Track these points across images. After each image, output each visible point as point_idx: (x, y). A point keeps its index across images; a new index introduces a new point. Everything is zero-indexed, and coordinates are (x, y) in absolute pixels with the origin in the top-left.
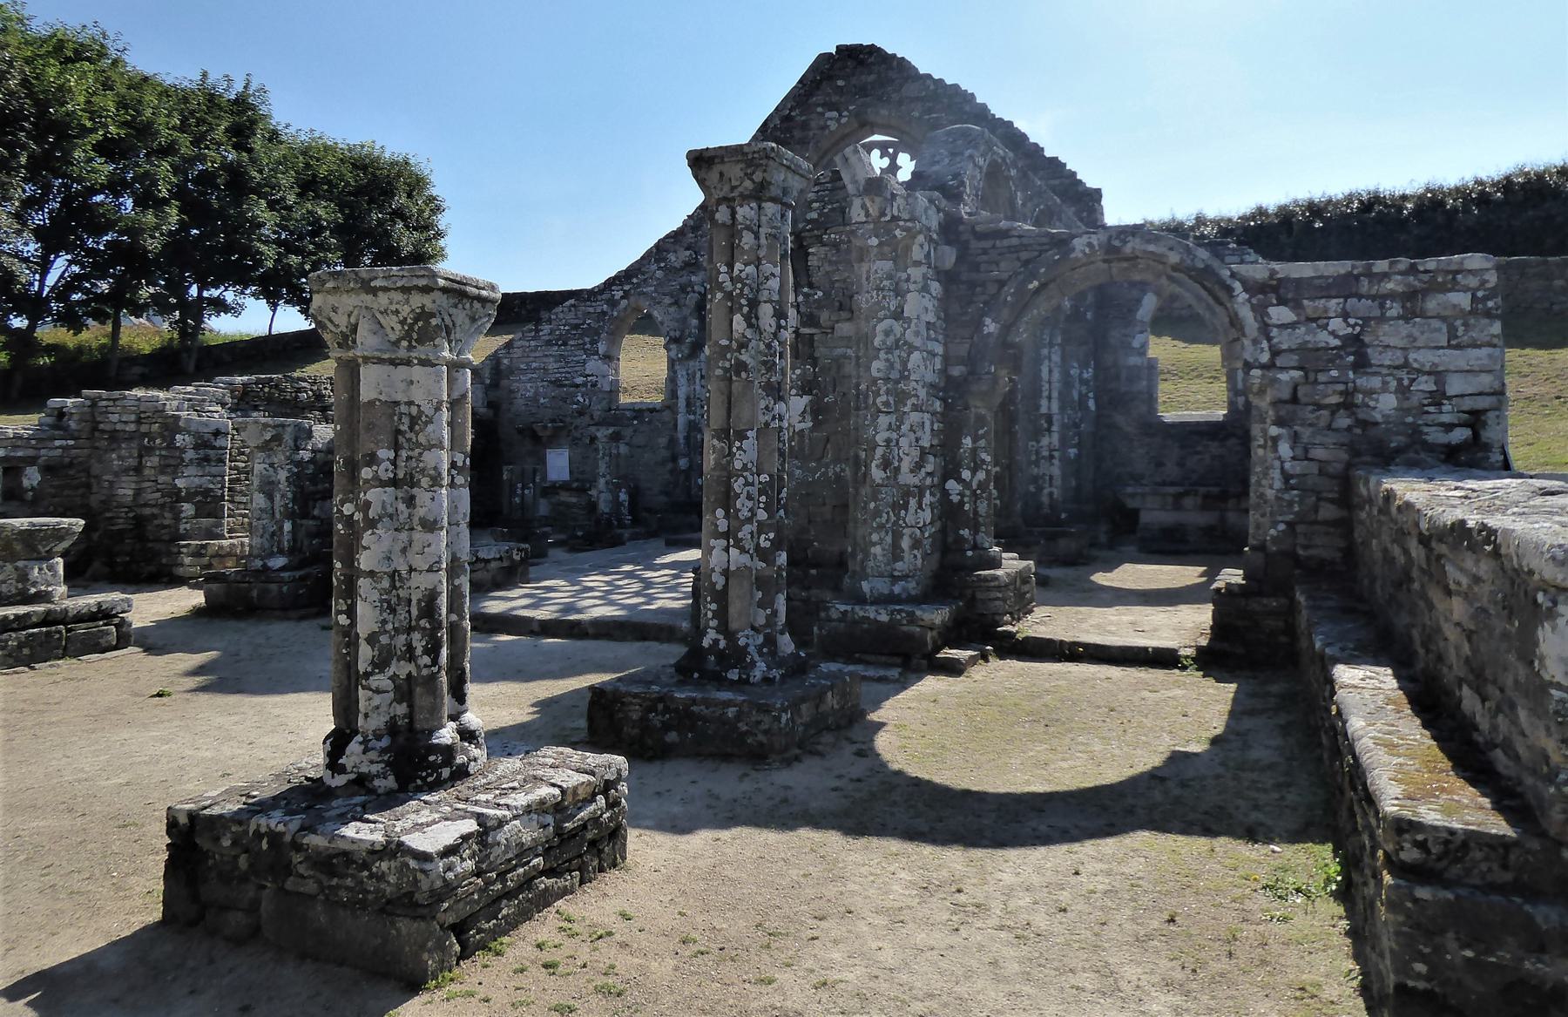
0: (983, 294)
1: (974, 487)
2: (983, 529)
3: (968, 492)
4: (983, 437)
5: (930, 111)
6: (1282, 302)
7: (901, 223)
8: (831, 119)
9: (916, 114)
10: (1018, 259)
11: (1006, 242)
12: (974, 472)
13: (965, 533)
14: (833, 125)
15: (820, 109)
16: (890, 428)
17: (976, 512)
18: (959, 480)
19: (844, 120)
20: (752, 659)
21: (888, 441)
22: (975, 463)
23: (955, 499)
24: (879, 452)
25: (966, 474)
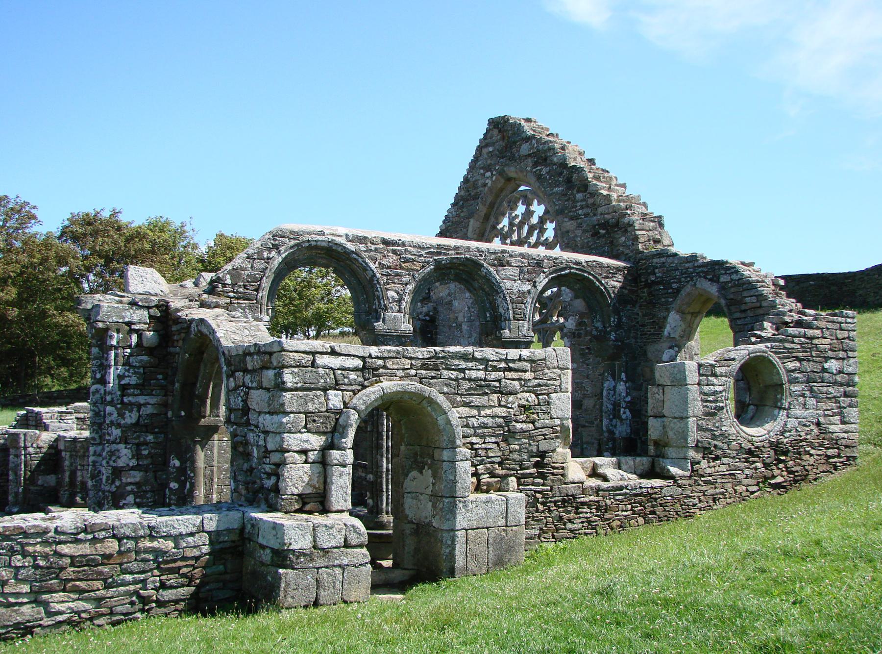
5: (536, 164)
8: (488, 178)
9: (529, 169)
14: (489, 182)
15: (482, 171)
16: (95, 454)
19: (494, 178)
21: (94, 462)
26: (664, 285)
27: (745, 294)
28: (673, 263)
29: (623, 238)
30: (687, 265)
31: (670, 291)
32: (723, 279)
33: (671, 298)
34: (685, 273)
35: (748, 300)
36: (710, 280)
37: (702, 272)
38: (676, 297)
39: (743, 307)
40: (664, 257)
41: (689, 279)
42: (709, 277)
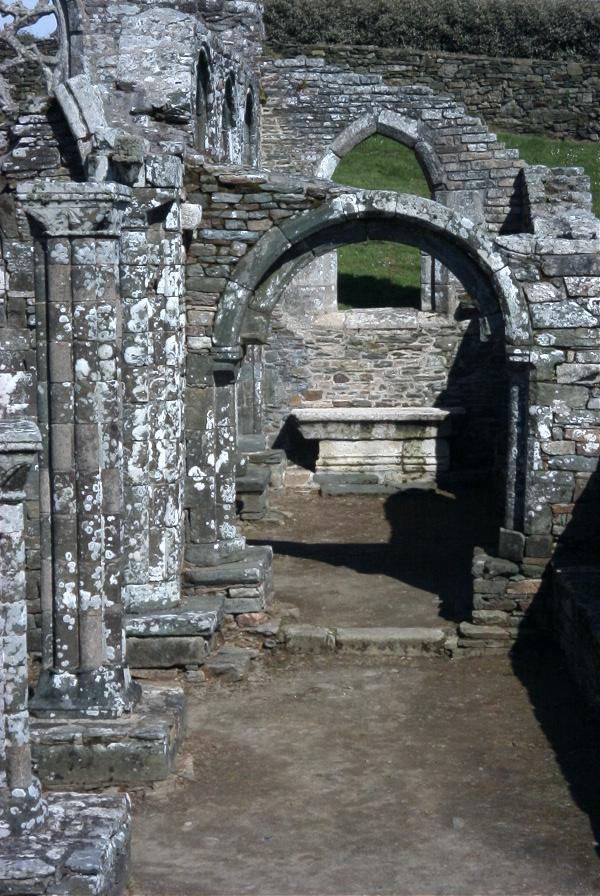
0: (229, 254)
1: (217, 471)
2: (227, 517)
3: (212, 479)
4: (226, 414)
6: (546, 278)
7: (158, 190)
10: (270, 218)
11: (257, 197)
12: (217, 455)
13: (213, 525)
17: (219, 499)
18: (204, 466)
20: (110, 693)
21: (145, 435)
22: (218, 443)
23: (200, 487)
24: (137, 447)
25: (211, 459)
26: (315, 114)
27: (466, 138)
28: (334, 82)
29: (229, 33)
30: (360, 89)
31: (326, 124)
32: (427, 115)
33: (329, 133)
34: (357, 100)
35: (472, 147)
36: (403, 114)
37: (390, 102)
38: (337, 133)
39: (463, 156)
40: (314, 72)
41: (364, 109)
42: (401, 110)
